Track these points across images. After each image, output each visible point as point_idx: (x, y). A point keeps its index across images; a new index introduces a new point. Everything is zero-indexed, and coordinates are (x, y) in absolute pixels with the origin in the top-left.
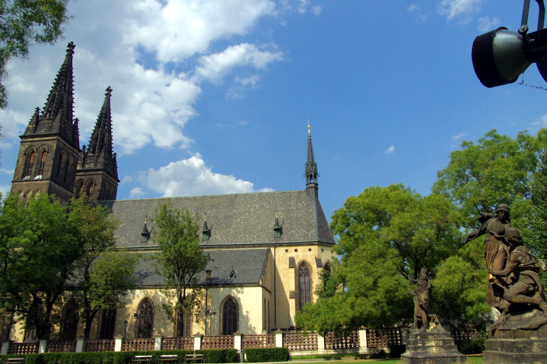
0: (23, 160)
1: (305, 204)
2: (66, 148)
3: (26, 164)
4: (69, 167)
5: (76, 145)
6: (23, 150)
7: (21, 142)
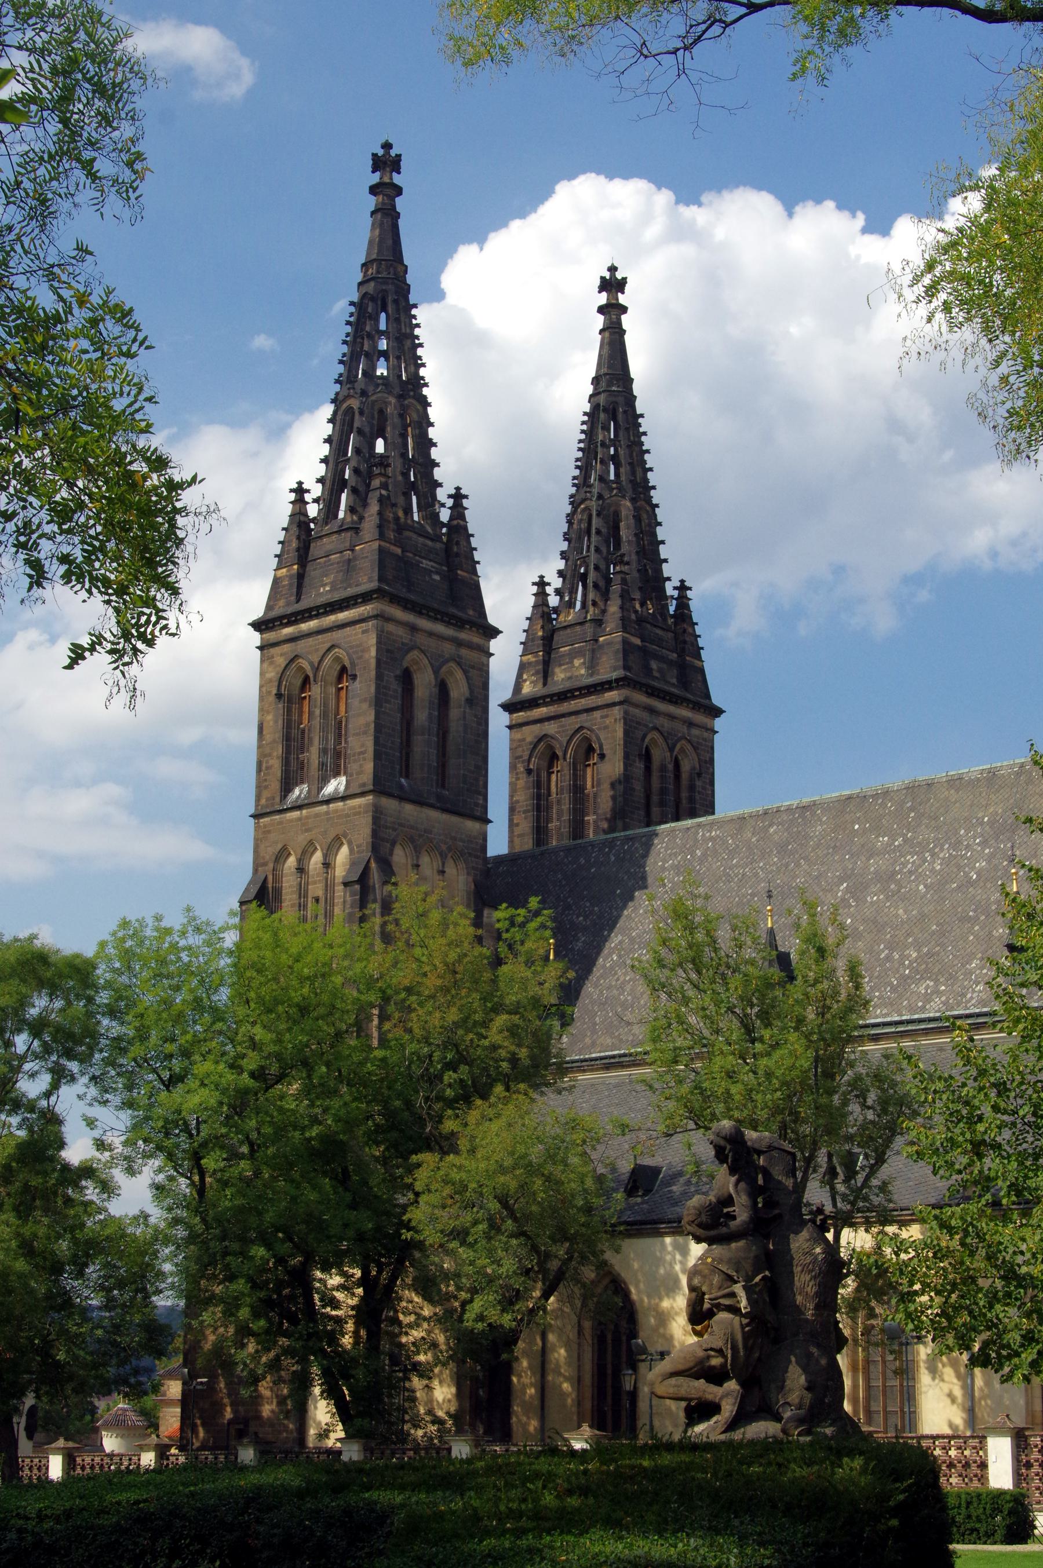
3: (287, 738)
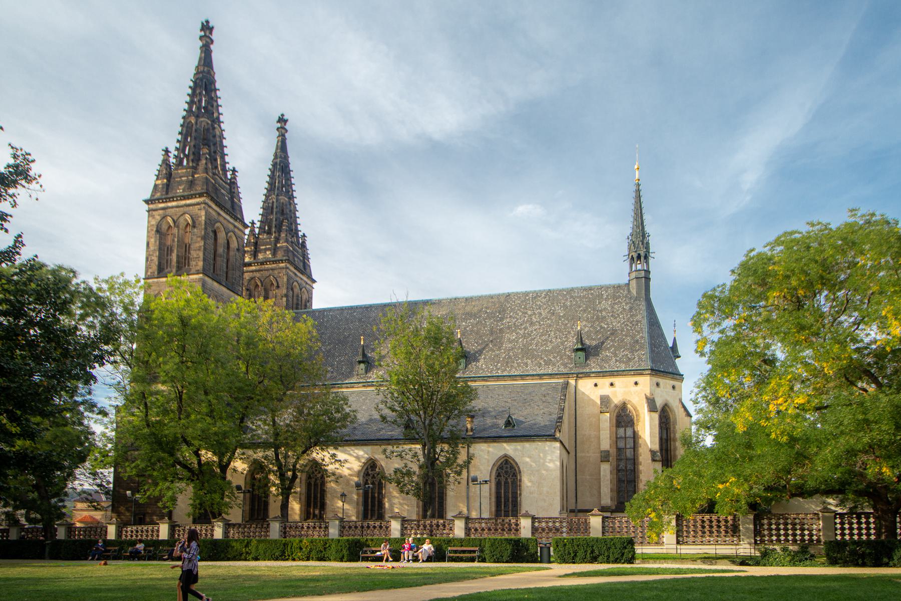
0: (156, 242)
1: (627, 307)
2: (221, 219)
4: (231, 253)
5: (239, 216)
6: (153, 225)
7: (148, 211)
